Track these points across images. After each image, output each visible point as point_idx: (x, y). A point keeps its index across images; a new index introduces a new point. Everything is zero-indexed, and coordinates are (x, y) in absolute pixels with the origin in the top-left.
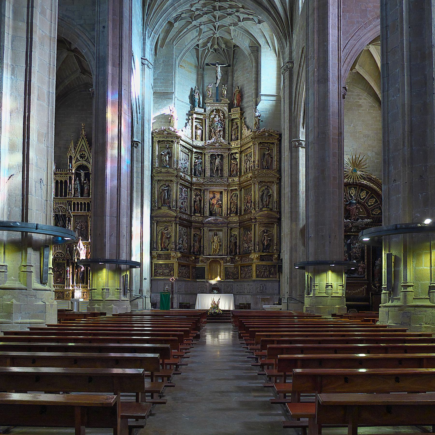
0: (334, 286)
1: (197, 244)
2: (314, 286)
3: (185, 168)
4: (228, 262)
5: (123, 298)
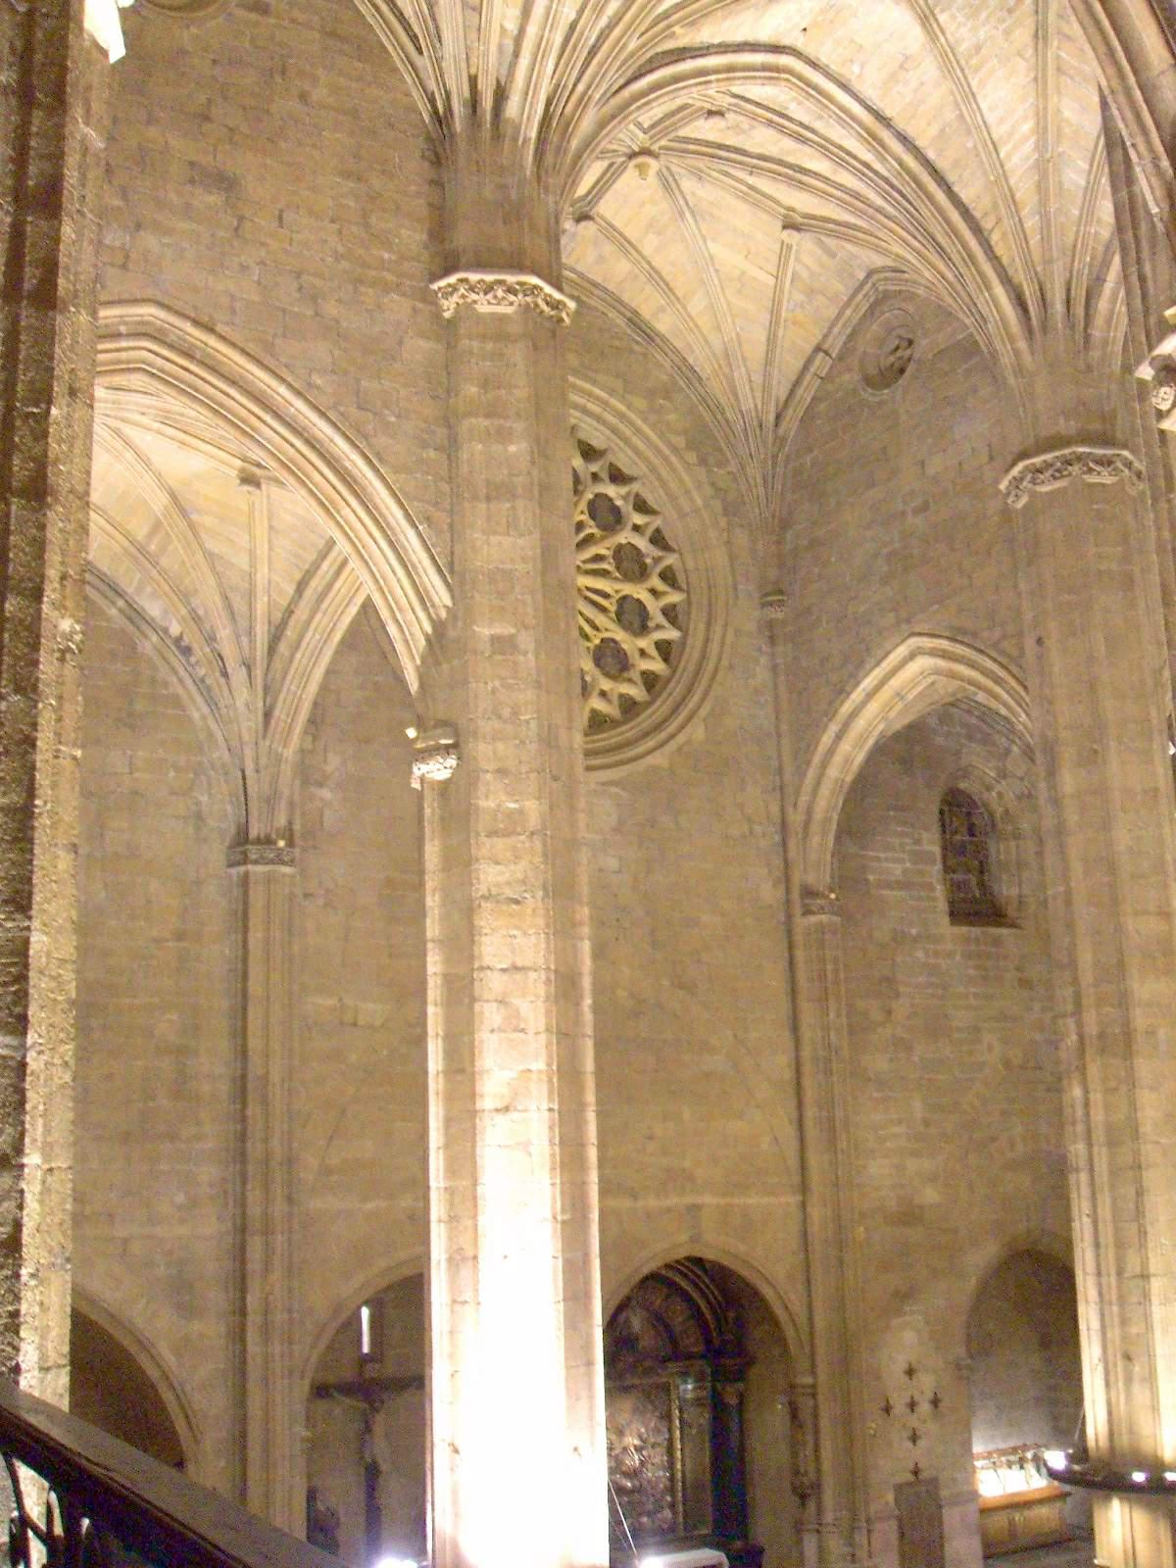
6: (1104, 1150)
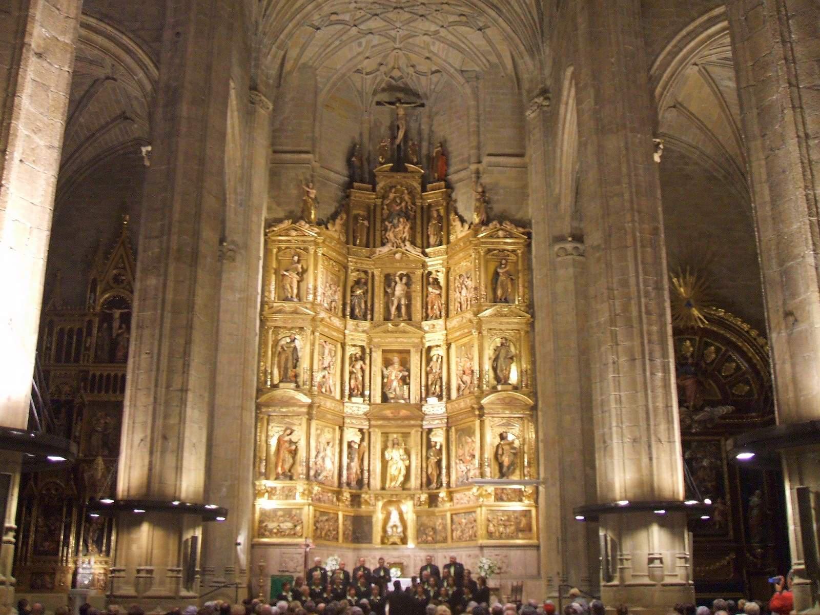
0: (667, 560)
2: (621, 560)
5: (184, 593)
6: (170, 314)
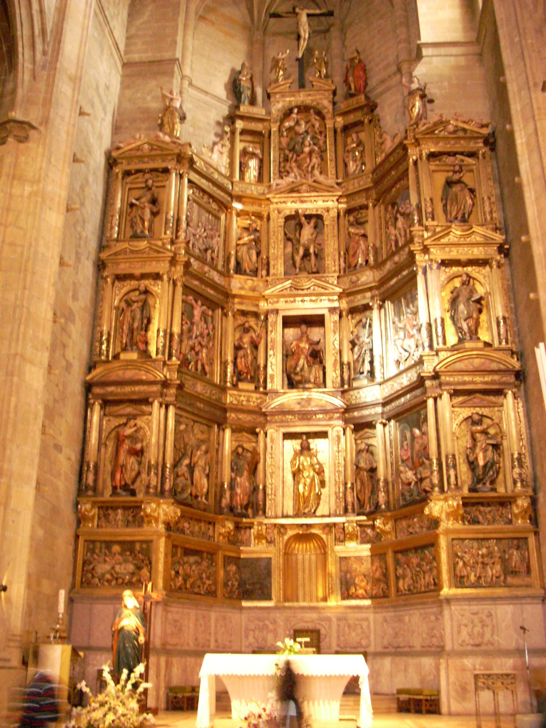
1: (243, 481)
3: (206, 250)
4: (351, 539)
